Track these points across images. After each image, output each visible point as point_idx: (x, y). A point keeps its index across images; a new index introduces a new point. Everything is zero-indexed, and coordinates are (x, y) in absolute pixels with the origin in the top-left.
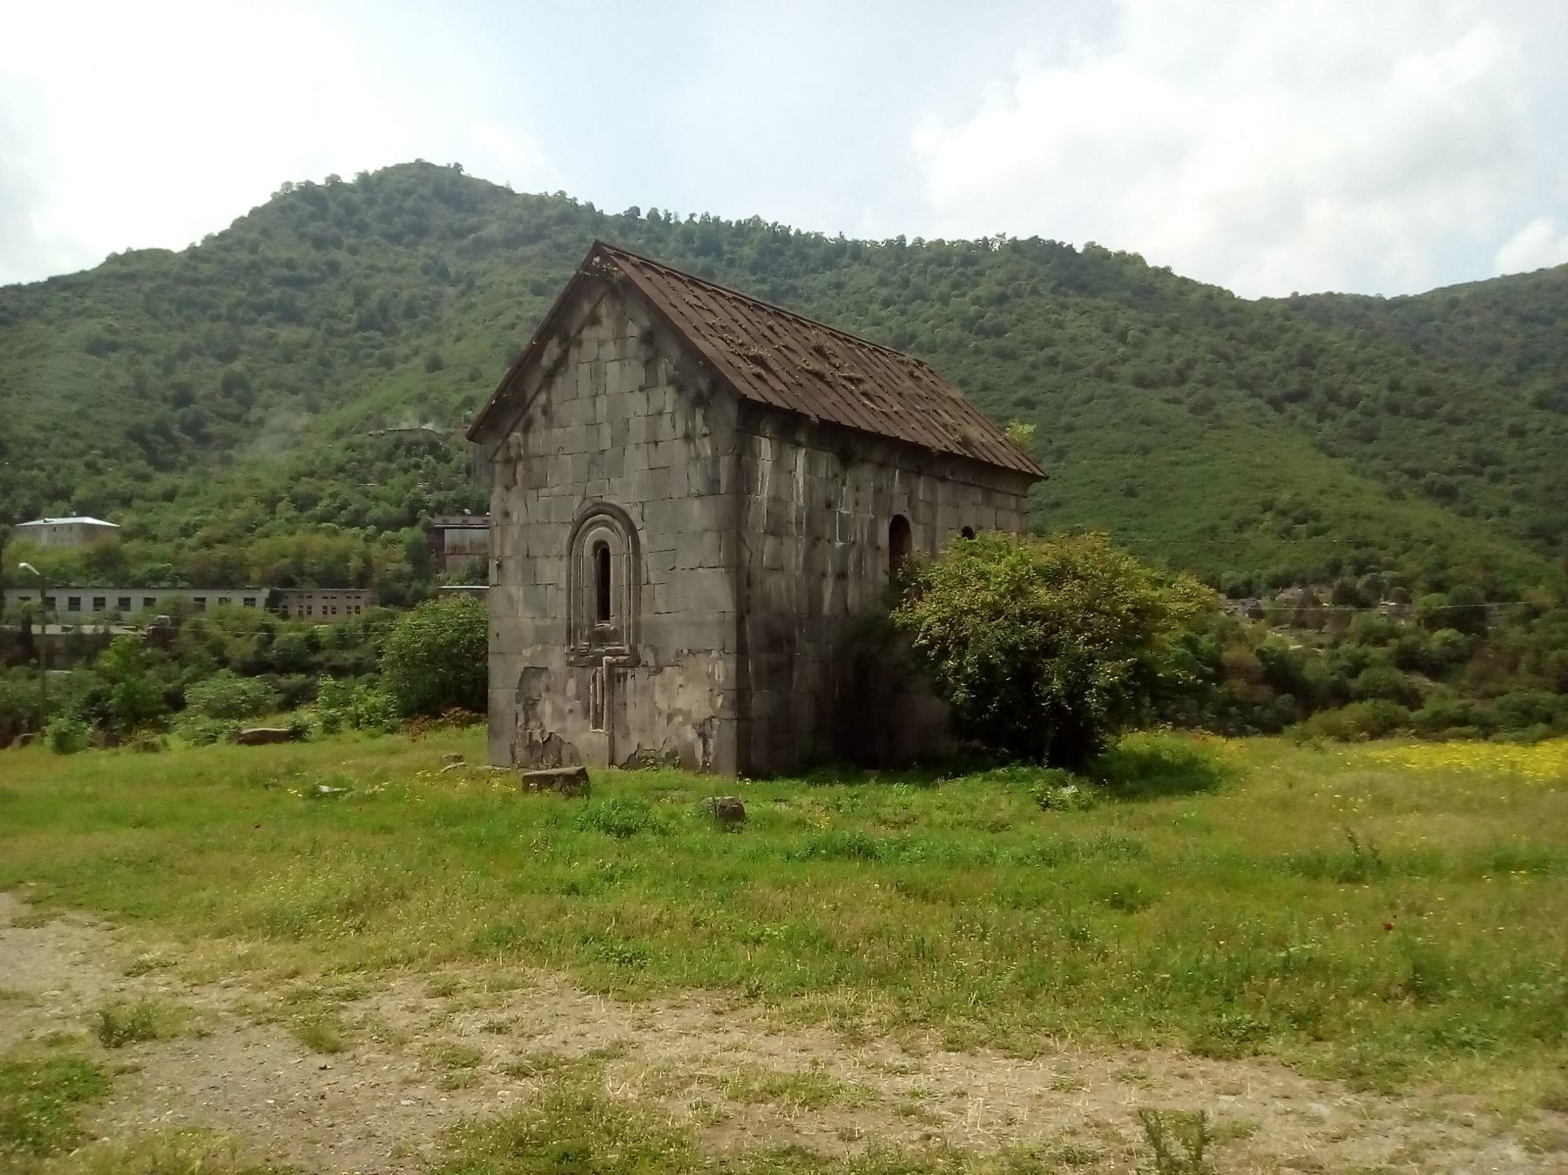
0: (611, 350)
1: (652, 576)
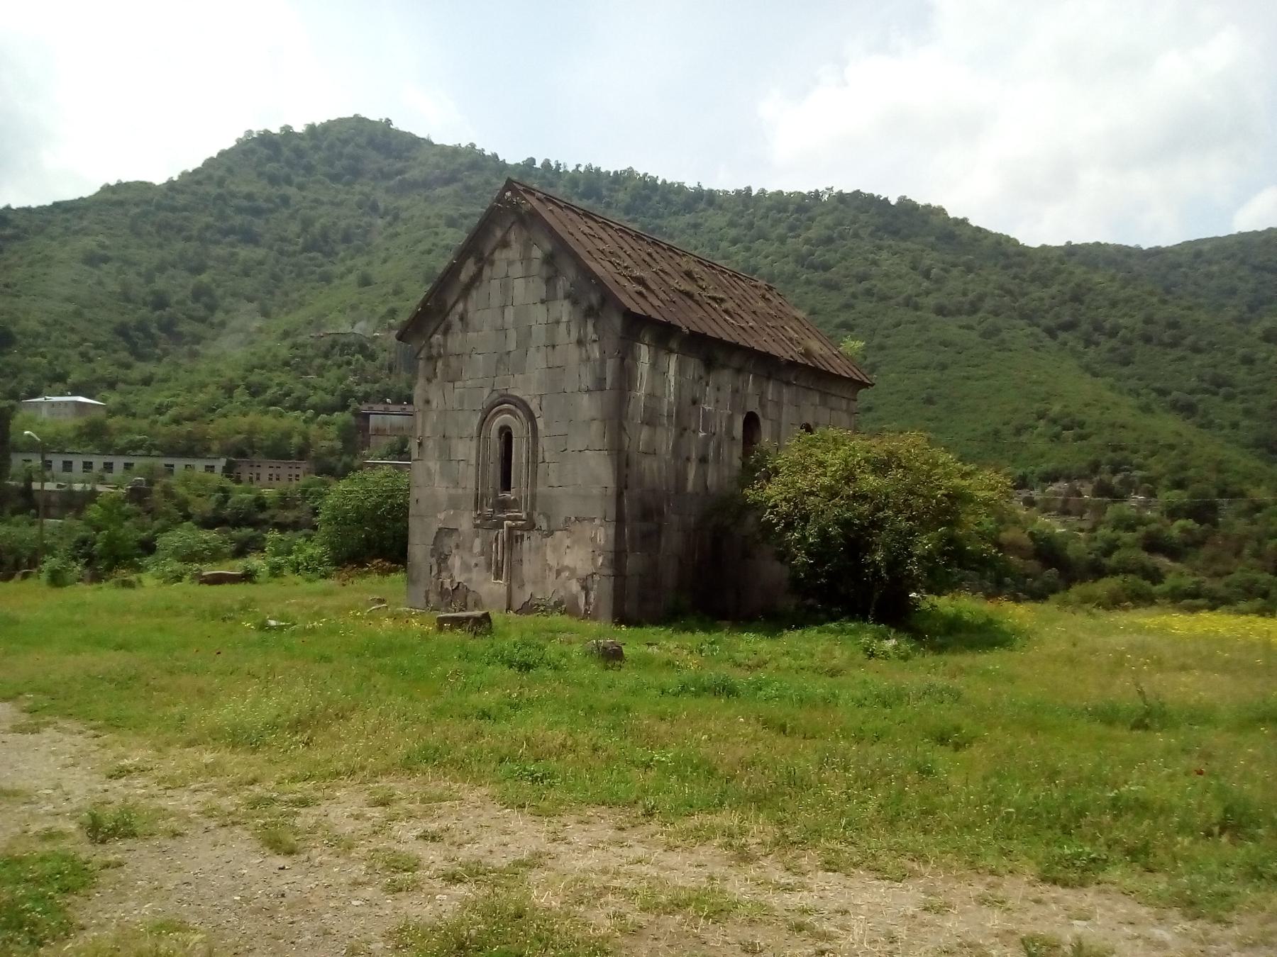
0: (518, 269)
1: (547, 454)
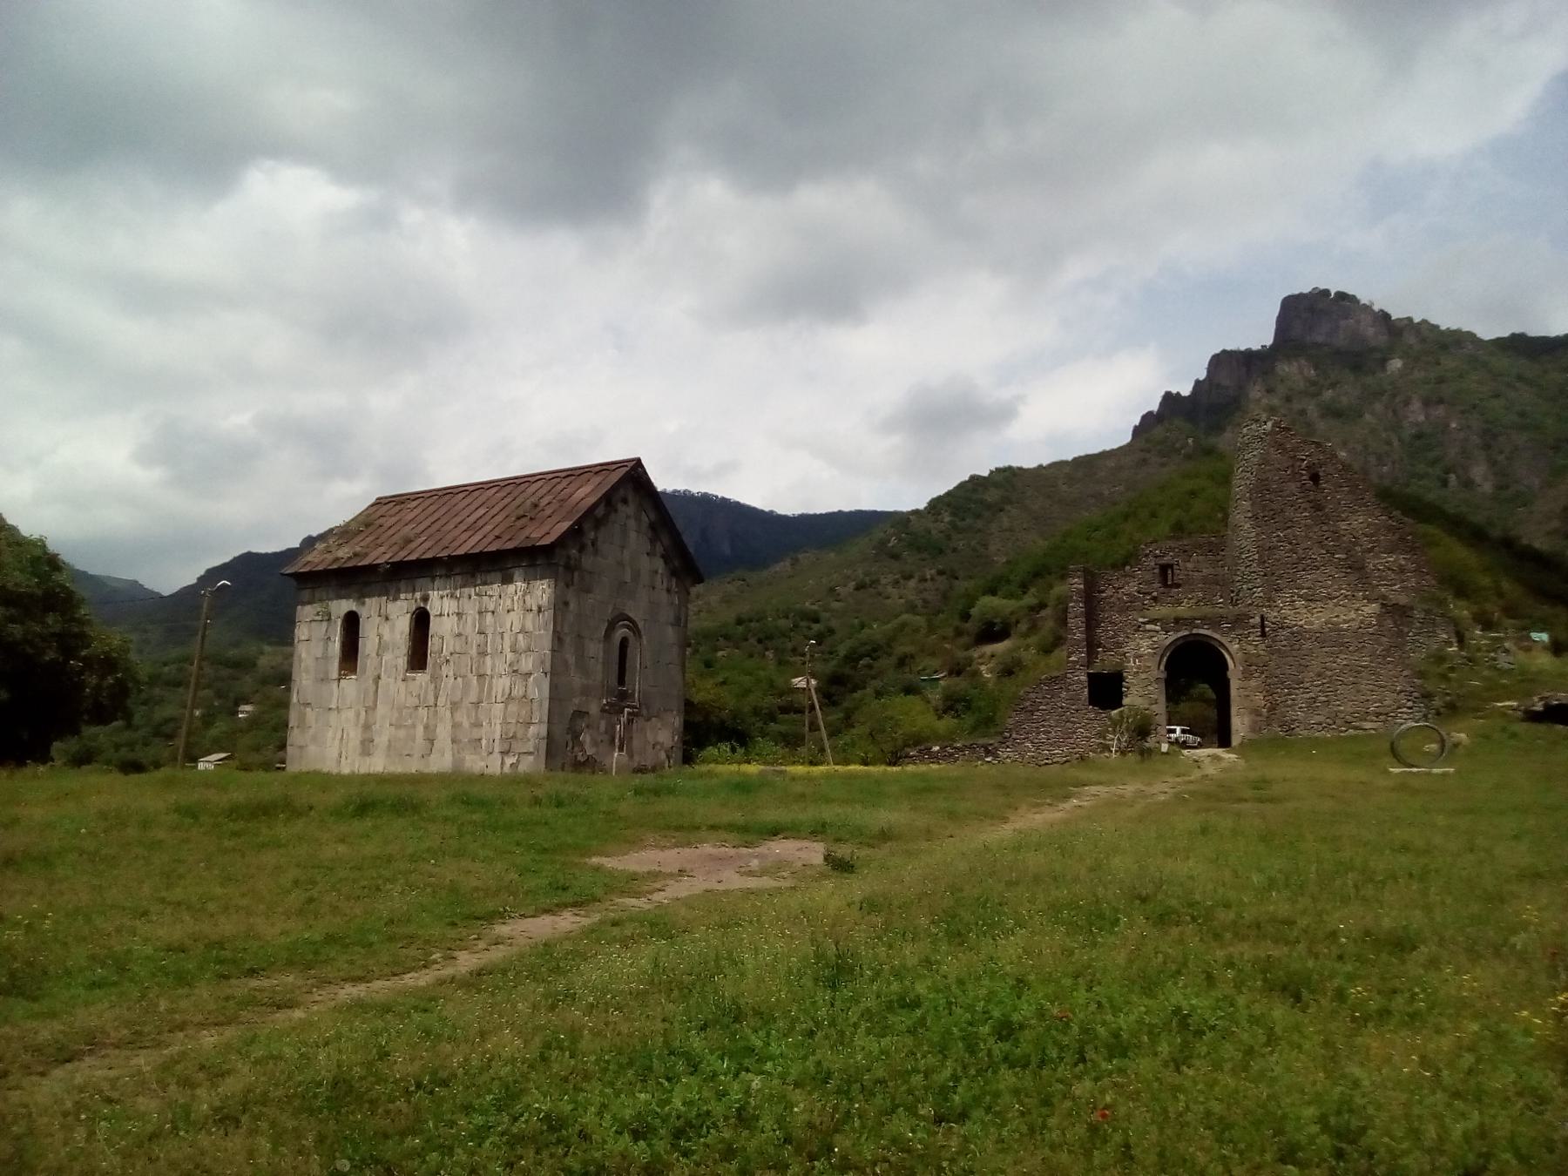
0: (632, 523)
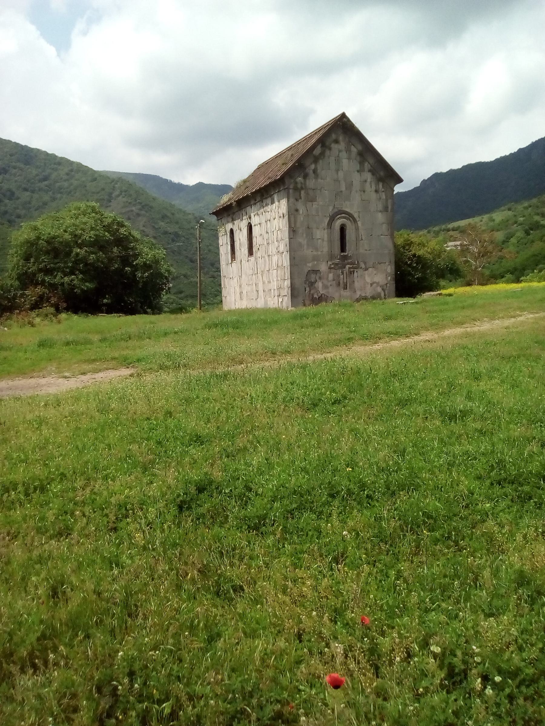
0: (344, 155)
